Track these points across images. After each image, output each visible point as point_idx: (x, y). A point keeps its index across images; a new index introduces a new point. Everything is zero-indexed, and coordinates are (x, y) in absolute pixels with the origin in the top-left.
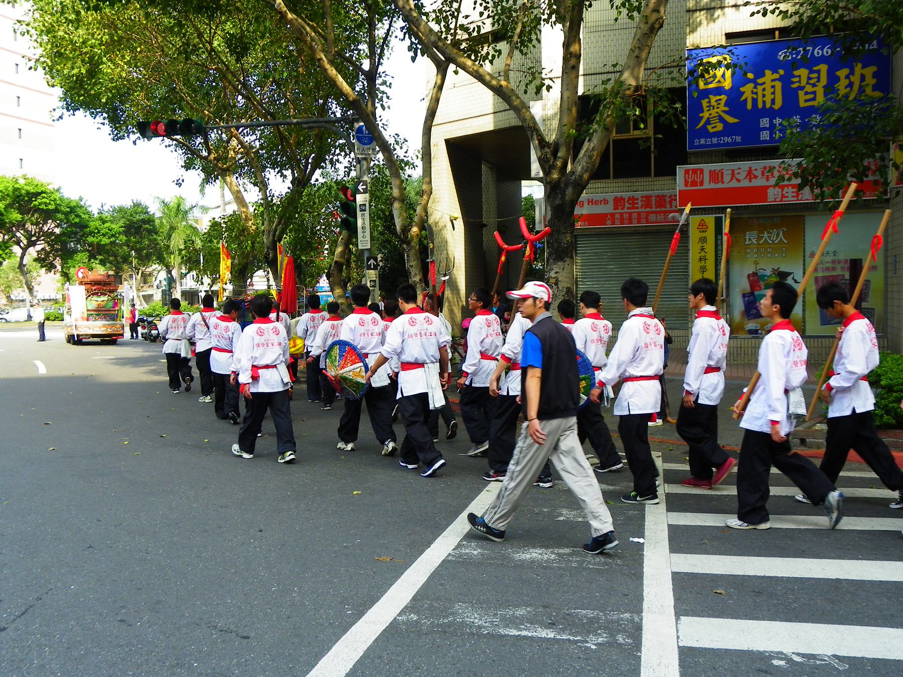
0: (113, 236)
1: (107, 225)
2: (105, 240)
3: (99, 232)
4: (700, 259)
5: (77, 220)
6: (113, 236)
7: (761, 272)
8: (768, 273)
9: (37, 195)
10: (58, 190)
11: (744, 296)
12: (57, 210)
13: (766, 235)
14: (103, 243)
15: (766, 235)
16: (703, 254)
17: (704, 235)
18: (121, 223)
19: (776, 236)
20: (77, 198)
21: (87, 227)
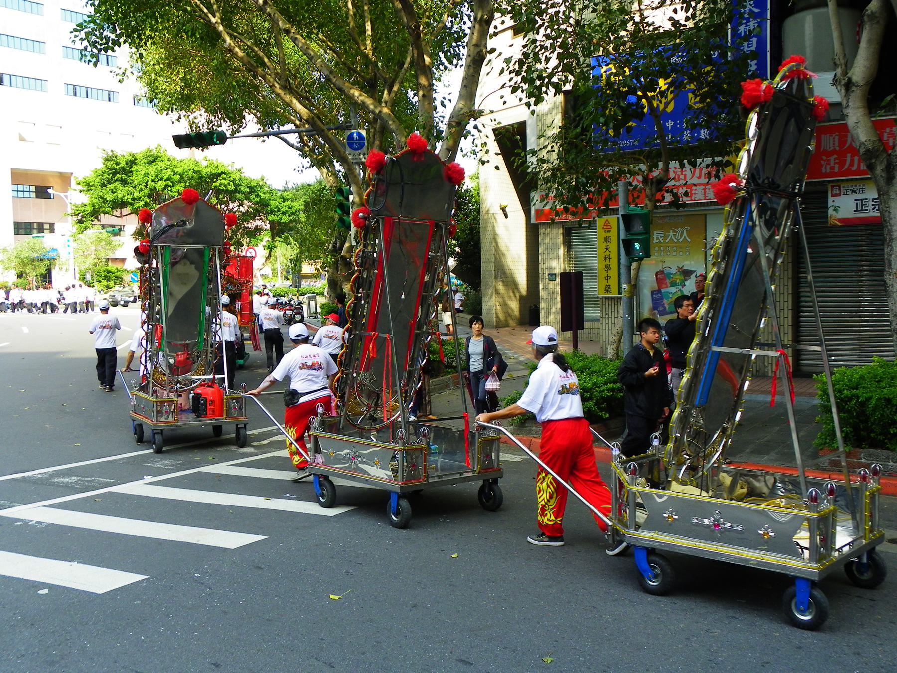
0: (293, 214)
1: (286, 203)
2: (285, 219)
3: (279, 210)
4: (605, 258)
5: (258, 199)
6: (293, 214)
7: (667, 270)
8: (674, 271)
9: (220, 175)
10: (239, 170)
11: (653, 293)
12: (236, 191)
13: (671, 234)
14: (283, 221)
15: (671, 234)
16: (607, 253)
17: (608, 234)
18: (302, 202)
19: (681, 235)
20: (259, 178)
21: (268, 205)
